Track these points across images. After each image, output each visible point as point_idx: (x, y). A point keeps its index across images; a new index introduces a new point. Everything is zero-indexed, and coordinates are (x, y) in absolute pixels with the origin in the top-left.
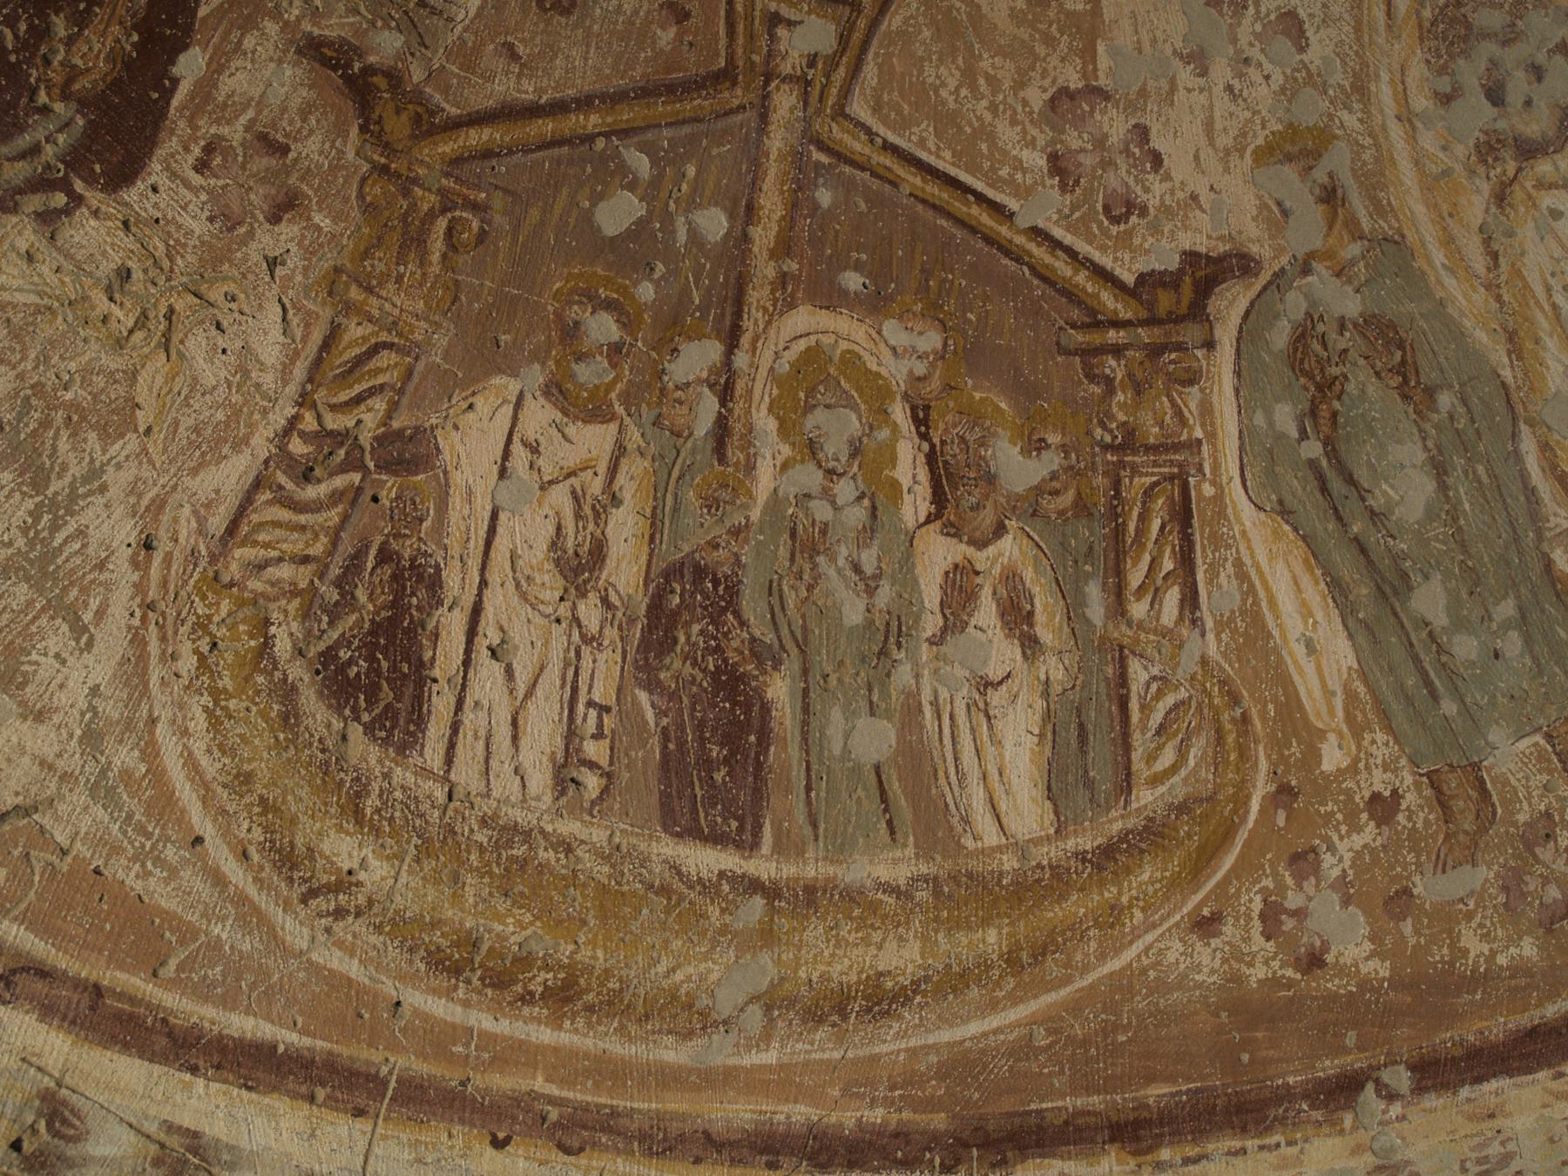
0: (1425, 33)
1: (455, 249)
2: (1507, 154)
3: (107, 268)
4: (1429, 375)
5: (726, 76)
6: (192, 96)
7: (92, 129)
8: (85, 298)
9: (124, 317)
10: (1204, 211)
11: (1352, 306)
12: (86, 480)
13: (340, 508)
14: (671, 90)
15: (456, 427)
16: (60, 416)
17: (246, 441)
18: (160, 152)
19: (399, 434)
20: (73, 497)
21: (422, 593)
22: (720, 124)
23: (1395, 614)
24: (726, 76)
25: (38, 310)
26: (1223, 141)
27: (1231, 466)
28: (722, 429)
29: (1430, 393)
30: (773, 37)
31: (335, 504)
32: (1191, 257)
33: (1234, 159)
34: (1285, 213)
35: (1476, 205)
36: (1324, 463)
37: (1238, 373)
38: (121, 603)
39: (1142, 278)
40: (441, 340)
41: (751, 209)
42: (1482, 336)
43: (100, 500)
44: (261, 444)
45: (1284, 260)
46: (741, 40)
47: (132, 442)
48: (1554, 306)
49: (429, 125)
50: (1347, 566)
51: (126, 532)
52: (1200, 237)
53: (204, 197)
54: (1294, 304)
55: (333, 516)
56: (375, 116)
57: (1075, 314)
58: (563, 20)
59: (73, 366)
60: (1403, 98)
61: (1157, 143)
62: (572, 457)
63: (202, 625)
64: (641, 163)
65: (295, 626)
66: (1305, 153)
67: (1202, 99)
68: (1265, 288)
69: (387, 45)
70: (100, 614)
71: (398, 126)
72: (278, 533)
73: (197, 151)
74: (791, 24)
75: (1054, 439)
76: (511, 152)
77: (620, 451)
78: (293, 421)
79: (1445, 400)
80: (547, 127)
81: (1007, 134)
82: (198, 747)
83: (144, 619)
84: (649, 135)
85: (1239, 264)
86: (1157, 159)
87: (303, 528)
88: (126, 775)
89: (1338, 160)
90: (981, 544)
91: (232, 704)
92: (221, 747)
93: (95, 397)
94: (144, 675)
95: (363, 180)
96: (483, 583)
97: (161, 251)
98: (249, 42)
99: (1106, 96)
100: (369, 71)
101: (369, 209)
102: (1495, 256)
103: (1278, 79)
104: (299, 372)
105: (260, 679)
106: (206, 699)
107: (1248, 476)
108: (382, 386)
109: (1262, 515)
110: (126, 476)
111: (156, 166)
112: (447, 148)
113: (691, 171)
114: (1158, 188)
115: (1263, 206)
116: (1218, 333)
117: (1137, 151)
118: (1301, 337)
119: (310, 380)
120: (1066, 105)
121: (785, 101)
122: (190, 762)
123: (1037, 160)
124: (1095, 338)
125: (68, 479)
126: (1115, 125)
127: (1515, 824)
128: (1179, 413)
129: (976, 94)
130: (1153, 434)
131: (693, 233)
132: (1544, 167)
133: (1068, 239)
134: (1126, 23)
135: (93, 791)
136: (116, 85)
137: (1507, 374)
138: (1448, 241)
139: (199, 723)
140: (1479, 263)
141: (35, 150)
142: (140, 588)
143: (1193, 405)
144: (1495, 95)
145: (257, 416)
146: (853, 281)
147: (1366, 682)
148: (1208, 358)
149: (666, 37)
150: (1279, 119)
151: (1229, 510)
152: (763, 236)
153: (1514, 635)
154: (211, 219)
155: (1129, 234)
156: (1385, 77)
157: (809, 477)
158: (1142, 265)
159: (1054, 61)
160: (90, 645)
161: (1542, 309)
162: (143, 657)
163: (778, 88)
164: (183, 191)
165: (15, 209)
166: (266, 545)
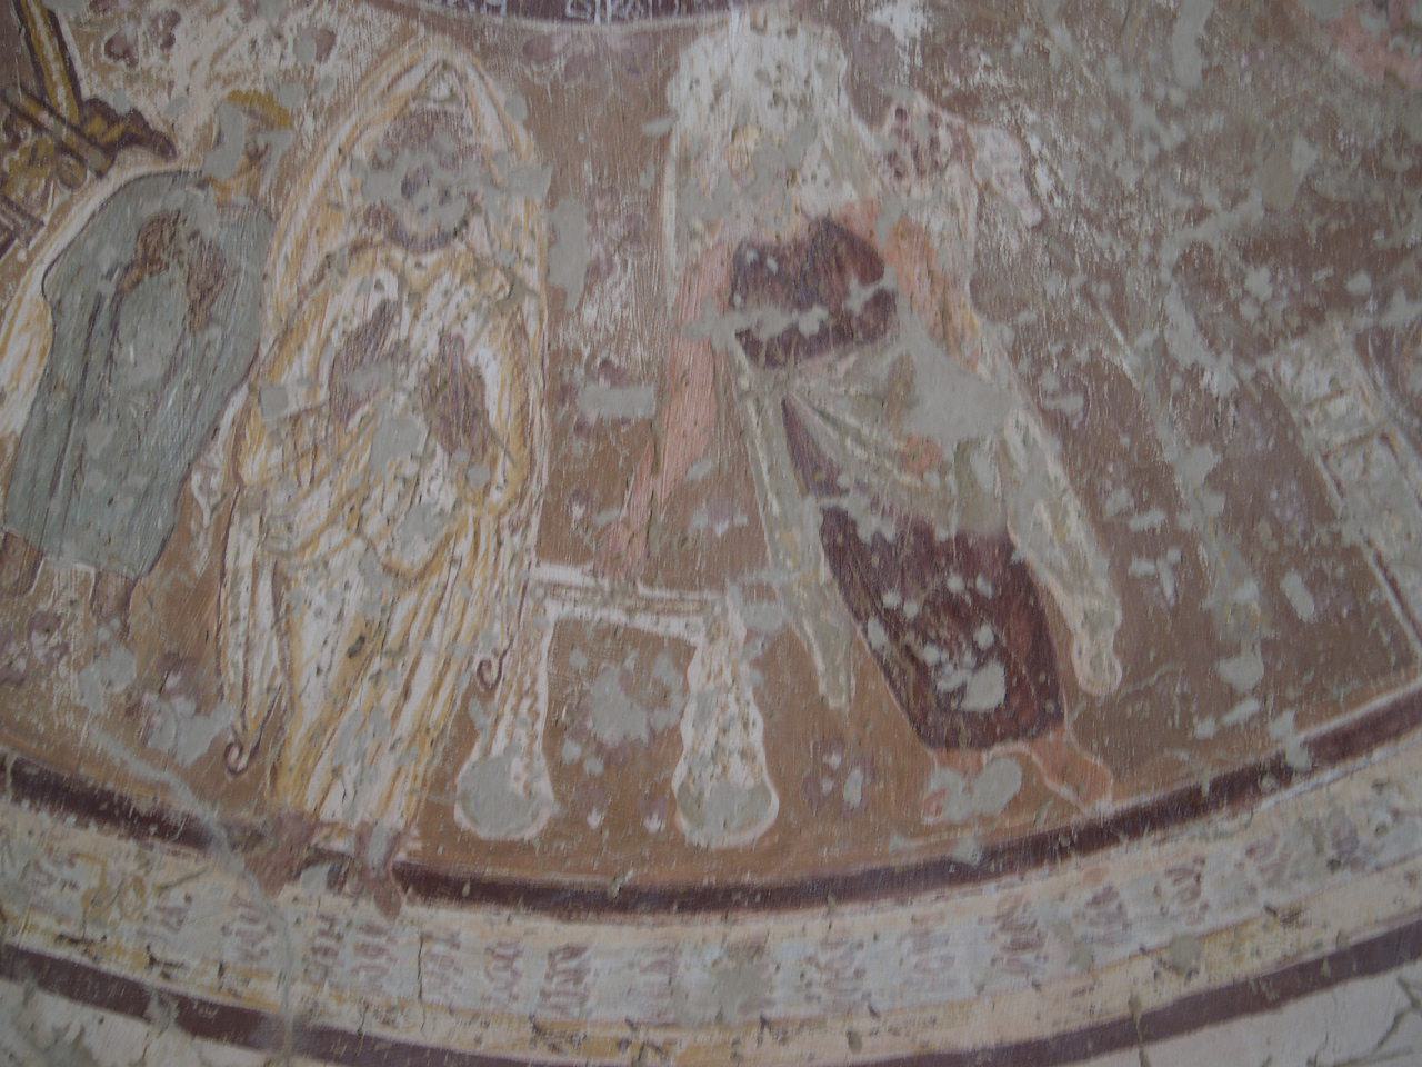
0: (402, 116)
2: (384, 228)
4: (218, 309)
10: (169, 95)
11: (210, 231)
23: (69, 426)
26: (220, 67)
27: (49, 254)
29: (210, 320)
32: (136, 115)
33: (218, 85)
34: (218, 141)
35: (337, 240)
36: (108, 302)
37: (102, 207)
39: (94, 102)
42: (270, 316)
45: (193, 168)
48: (328, 339)
50: (67, 371)
52: (153, 109)
54: (176, 199)
57: (32, 84)
60: (353, 140)
61: (178, 33)
66: (264, 119)
67: (229, 31)
68: (166, 174)
79: (215, 332)
85: (164, 146)
86: (169, 42)
89: (281, 142)
102: (321, 277)
103: (289, 63)
107: (54, 268)
109: (41, 299)
115: (209, 126)
117: (161, 27)
118: (160, 221)
124: (32, 108)
127: (35, 607)
130: (17, 194)
132: (398, 254)
133: (68, 37)
137: (264, 350)
138: (302, 245)
140: (308, 274)
143: (58, 201)
144: (408, 189)
147: (18, 445)
148: (92, 181)
150: (267, 89)
151: (23, 281)
153: (131, 501)
155: (111, 69)
156: (354, 118)
158: (99, 92)
161: (319, 333)
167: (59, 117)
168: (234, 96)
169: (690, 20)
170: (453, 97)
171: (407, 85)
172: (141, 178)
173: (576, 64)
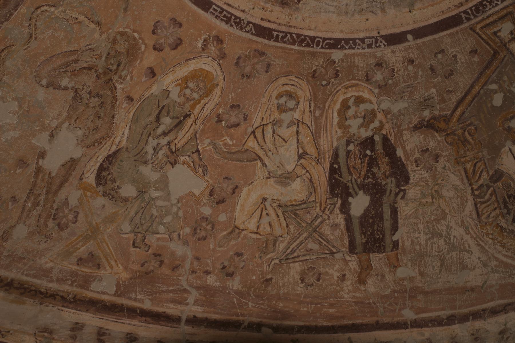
1: (473, 135)
3: (419, 195)
5: (496, 53)
6: (405, 156)
7: (396, 178)
8: (421, 202)
12: (447, 229)
13: (494, 196)
14: (487, 67)
15: (502, 165)
16: (434, 223)
17: (467, 199)
18: (409, 170)
19: (493, 174)
20: (448, 233)
22: (504, 63)
24: (496, 53)
25: (415, 212)
30: (498, 37)
31: (492, 196)
38: (471, 242)
40: (485, 153)
43: (452, 230)
44: (470, 198)
46: (492, 44)
47: (449, 217)
49: (447, 120)
51: (461, 231)
53: (423, 170)
55: (494, 198)
56: (437, 127)
58: (453, 76)
59: (429, 214)
63: (487, 234)
64: (494, 87)
65: (503, 221)
69: (426, 114)
70: (469, 246)
71: (442, 125)
72: (487, 209)
73: (414, 164)
74: (500, 31)
76: (467, 109)
78: (472, 189)
80: (469, 98)
82: (504, 252)
83: (477, 241)
84: (491, 80)
87: (490, 204)
88: (496, 266)
91: (504, 241)
92: (508, 249)
93: (437, 215)
94: (485, 249)
95: (446, 140)
97: (424, 184)
98: (405, 138)
100: (428, 121)
101: (451, 144)
105: (505, 234)
106: (499, 244)
108: (482, 171)
110: (453, 222)
111: (410, 173)
112: (455, 119)
113: (505, 78)
119: (469, 180)
122: (505, 256)
125: (445, 231)
135: (493, 272)
136: (392, 168)
139: (501, 249)
141: (391, 191)
142: (472, 237)
145: (465, 194)
149: (476, 59)
154: (427, 172)
160: (472, 252)
162: (482, 247)
163: (509, 45)
164: (419, 172)
166: (487, 212)
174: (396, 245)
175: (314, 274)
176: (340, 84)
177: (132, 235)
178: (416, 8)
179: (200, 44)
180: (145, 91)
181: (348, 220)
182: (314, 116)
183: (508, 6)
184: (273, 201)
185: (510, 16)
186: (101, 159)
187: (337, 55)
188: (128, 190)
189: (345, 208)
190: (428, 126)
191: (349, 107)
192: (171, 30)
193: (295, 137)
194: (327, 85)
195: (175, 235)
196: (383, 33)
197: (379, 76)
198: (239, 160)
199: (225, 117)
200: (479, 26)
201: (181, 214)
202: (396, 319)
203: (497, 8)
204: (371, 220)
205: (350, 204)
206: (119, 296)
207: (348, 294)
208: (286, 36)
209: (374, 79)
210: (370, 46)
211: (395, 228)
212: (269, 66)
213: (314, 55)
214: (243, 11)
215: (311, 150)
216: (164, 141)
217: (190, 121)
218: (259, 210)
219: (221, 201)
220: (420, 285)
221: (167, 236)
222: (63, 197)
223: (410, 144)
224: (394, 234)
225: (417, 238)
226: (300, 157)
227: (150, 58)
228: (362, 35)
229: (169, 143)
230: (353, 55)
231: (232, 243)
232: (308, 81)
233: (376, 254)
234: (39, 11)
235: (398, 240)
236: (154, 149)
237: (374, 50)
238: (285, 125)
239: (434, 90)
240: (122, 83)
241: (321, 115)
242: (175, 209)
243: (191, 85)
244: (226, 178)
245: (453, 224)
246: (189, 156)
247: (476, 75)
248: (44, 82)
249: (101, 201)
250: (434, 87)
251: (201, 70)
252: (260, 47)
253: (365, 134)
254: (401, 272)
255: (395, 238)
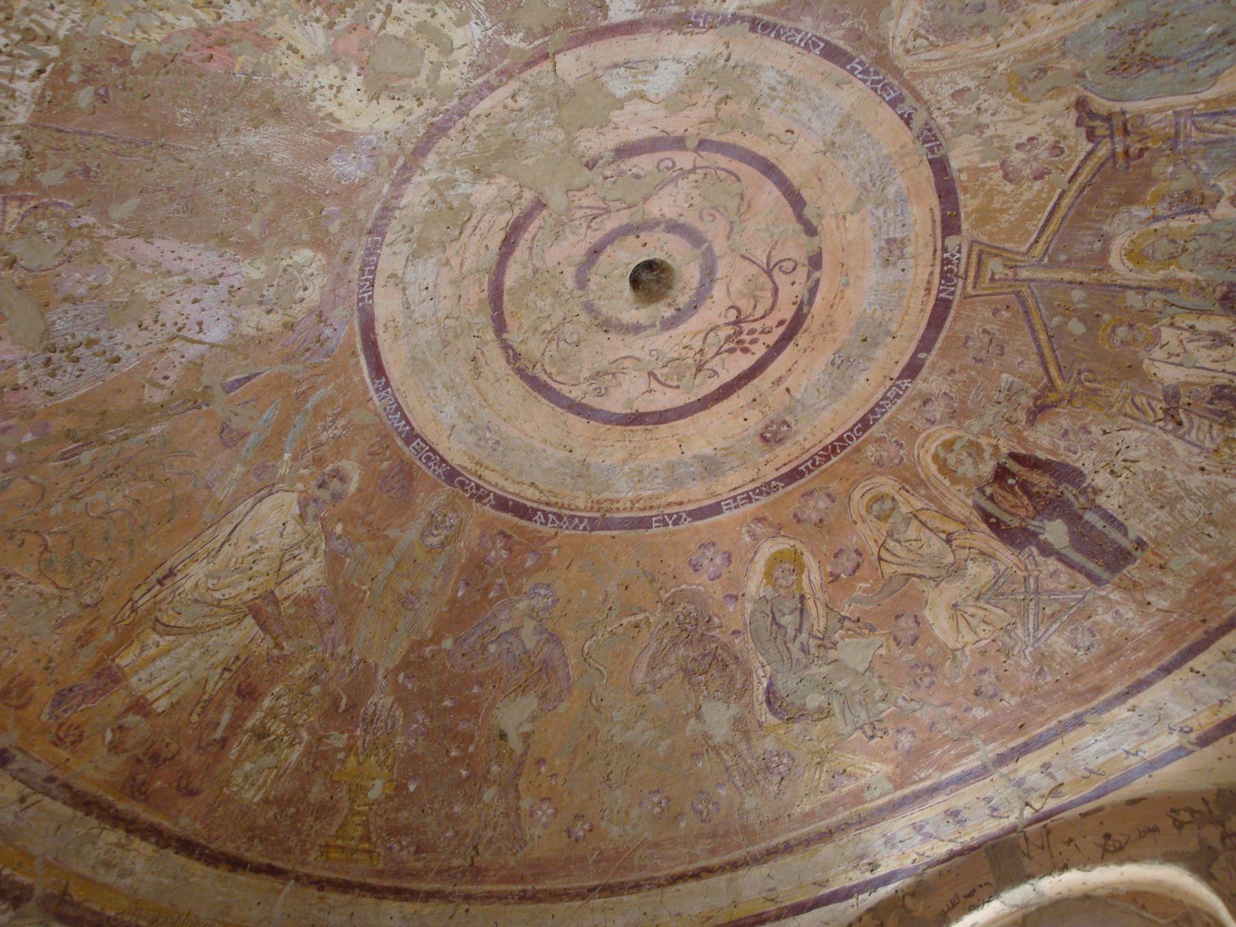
3: (1109, 476)
5: (1018, 294)
7: (1068, 482)
9: (1126, 473)
19: (1165, 397)
21: (1226, 391)
24: (1018, 294)
26: (1019, 114)
28: (1161, 290)
32: (1078, 124)
38: (1222, 478)
40: (1130, 383)
41: (1070, 282)
44: (1169, 437)
47: (1168, 474)
52: (1068, 123)
57: (1109, 164)
60: (988, 47)
61: (1024, 139)
62: (1174, 342)
64: (1056, 320)
67: (999, 125)
71: (1053, 397)
75: (1170, 169)
77: (1172, 325)
78: (1161, 428)
80: (1047, 351)
81: (1027, 196)
85: (1081, 104)
86: (1031, 139)
90: (1220, 195)
96: (1224, 371)
99: (1003, 164)
101: (1084, 405)
103: (985, 96)
104: (1143, 426)
114: (1045, 137)
115: (1051, 98)
116: (1118, 109)
120: (1011, 176)
121: (1024, 274)
123: (1037, 185)
126: (1017, 157)
128: (1159, 121)
129: (1012, 207)
131: (1083, 301)
133: (1073, 169)
134: (969, 157)
136: (1052, 476)
141: (1074, 495)
142: (1217, 474)
146: (1098, 245)
152: (1079, 277)
155: (1068, 147)
157: (1184, 259)
159: (992, 182)
165: (1094, 501)
167: (1113, 143)
168: (1026, 100)
169: (758, 15)
170: (917, 36)
171: (937, 54)
172: (1108, 99)
173: (837, 19)
174: (1140, 544)
175: (1083, 635)
176: (913, 448)
177: (859, 732)
178: (894, 329)
179: (747, 539)
180: (743, 615)
181: (1061, 558)
182: (923, 496)
183: (970, 250)
184: (965, 600)
185: (984, 256)
186: (762, 698)
187: (876, 430)
188: (814, 700)
189: (1047, 550)
190: (1039, 411)
191: (945, 460)
192: (709, 554)
193: (924, 529)
194: (902, 460)
195: (901, 702)
196: (895, 375)
197: (937, 409)
198: (892, 593)
199: (838, 570)
200: (969, 289)
201: (885, 680)
202: (1226, 616)
203: (963, 261)
204: (1084, 538)
205: (1046, 542)
206: (901, 787)
207: (1141, 625)
208: (814, 461)
209: (938, 416)
210: (898, 396)
211: (1122, 528)
212: (829, 496)
213: (857, 450)
214: (754, 480)
215: (951, 526)
216: (804, 636)
217: (810, 603)
218: (961, 620)
219: (915, 639)
220: (1213, 564)
221: (893, 708)
222: (761, 751)
223: (1043, 439)
224: (1126, 534)
225: (1157, 519)
226: (948, 541)
227: (717, 591)
228: (879, 395)
229: (811, 635)
230: (892, 417)
231: (965, 666)
232: (881, 474)
233: (1130, 567)
234: (586, 650)
235: (1139, 538)
236: (803, 650)
237: (908, 393)
238: (902, 527)
239: (1004, 376)
240: (714, 629)
241: (927, 487)
242: (876, 681)
243: (778, 573)
244: (897, 617)
245: (1180, 477)
246: (841, 628)
247: (1027, 329)
248: (649, 688)
249: (797, 727)
250: (1002, 372)
251: (773, 555)
252: (802, 491)
253: (988, 468)
254: (1175, 565)
255: (1132, 535)
